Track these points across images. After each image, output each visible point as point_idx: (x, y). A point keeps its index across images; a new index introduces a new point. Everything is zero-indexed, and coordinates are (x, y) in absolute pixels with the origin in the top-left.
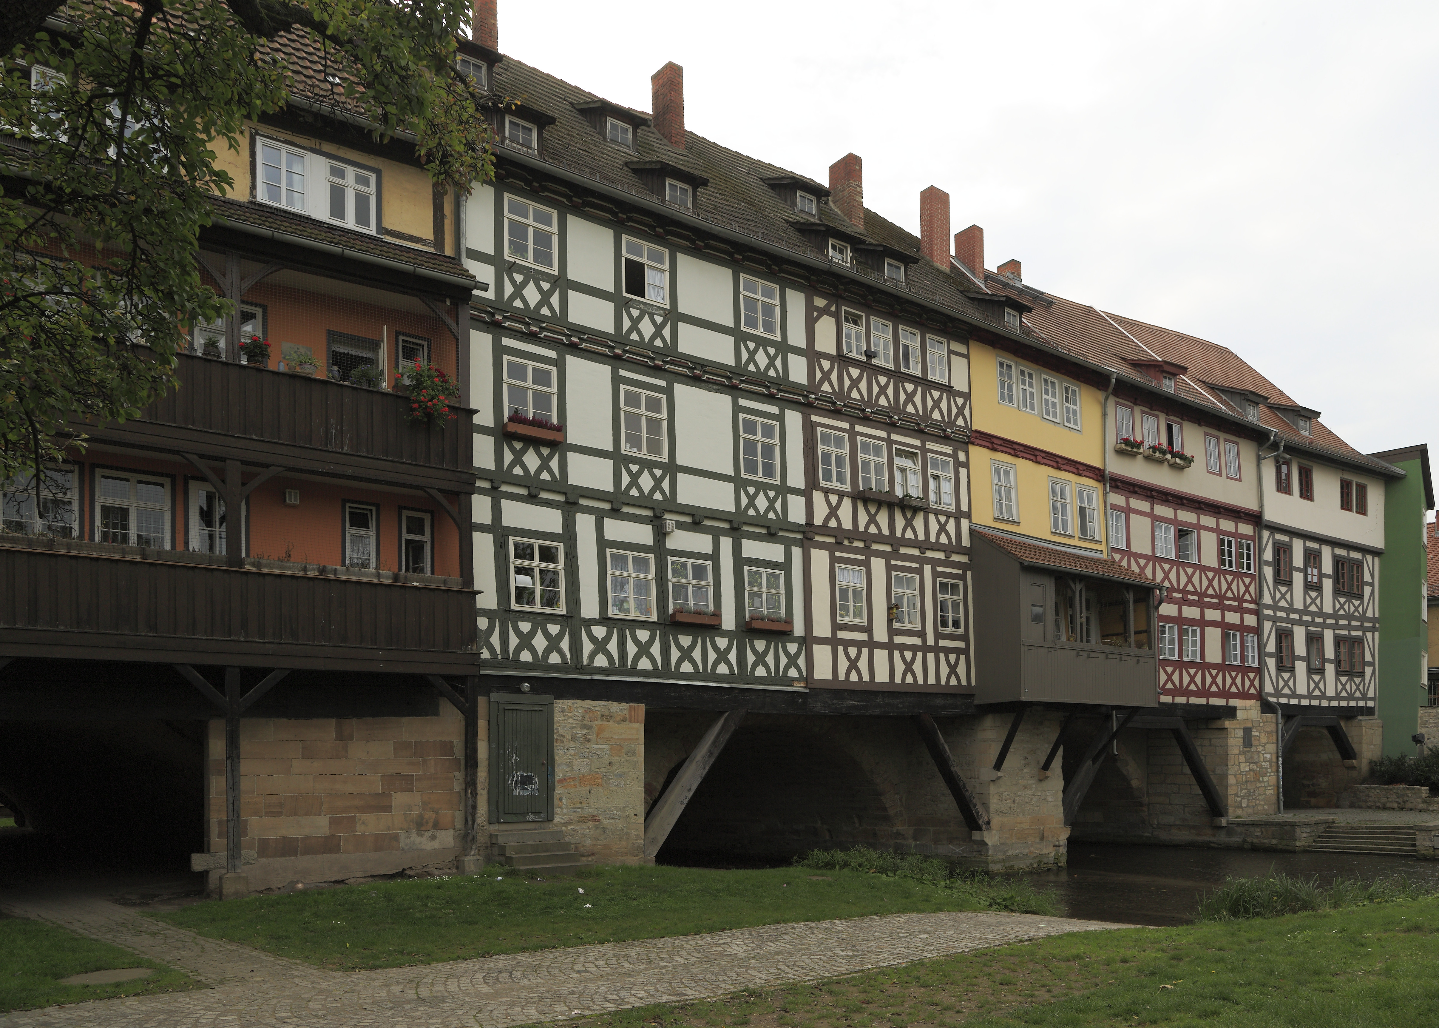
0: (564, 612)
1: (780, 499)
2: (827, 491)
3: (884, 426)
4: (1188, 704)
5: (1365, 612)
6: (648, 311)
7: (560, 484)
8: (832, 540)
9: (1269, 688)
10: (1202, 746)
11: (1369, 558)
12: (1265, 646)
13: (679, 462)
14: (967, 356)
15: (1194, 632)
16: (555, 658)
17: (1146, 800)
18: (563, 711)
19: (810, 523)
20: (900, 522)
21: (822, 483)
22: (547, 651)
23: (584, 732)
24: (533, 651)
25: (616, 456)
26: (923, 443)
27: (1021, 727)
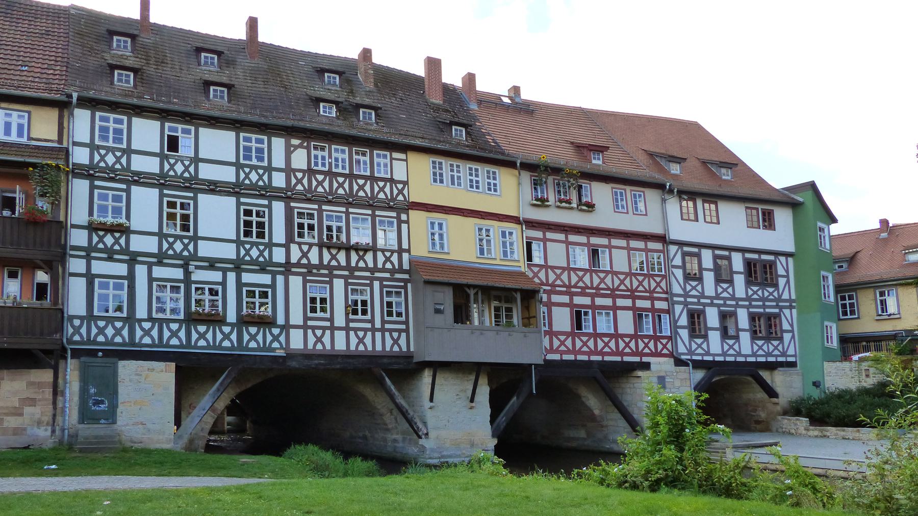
0: (126, 316)
1: (267, 249)
2: (300, 244)
3: (343, 204)
4: (603, 361)
5: (780, 296)
6: (181, 159)
7: (125, 251)
8: (305, 270)
9: (682, 349)
10: (630, 388)
11: (783, 259)
12: (676, 322)
13: (199, 235)
14: (406, 160)
15: (608, 314)
16: (118, 339)
17: (605, 423)
18: (124, 366)
19: (288, 262)
20: (354, 257)
21: (297, 239)
22: (114, 336)
23: (137, 377)
24: (106, 336)
25: (161, 235)
26: (374, 212)
27: (437, 374)
